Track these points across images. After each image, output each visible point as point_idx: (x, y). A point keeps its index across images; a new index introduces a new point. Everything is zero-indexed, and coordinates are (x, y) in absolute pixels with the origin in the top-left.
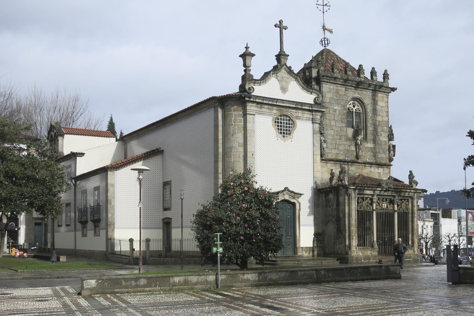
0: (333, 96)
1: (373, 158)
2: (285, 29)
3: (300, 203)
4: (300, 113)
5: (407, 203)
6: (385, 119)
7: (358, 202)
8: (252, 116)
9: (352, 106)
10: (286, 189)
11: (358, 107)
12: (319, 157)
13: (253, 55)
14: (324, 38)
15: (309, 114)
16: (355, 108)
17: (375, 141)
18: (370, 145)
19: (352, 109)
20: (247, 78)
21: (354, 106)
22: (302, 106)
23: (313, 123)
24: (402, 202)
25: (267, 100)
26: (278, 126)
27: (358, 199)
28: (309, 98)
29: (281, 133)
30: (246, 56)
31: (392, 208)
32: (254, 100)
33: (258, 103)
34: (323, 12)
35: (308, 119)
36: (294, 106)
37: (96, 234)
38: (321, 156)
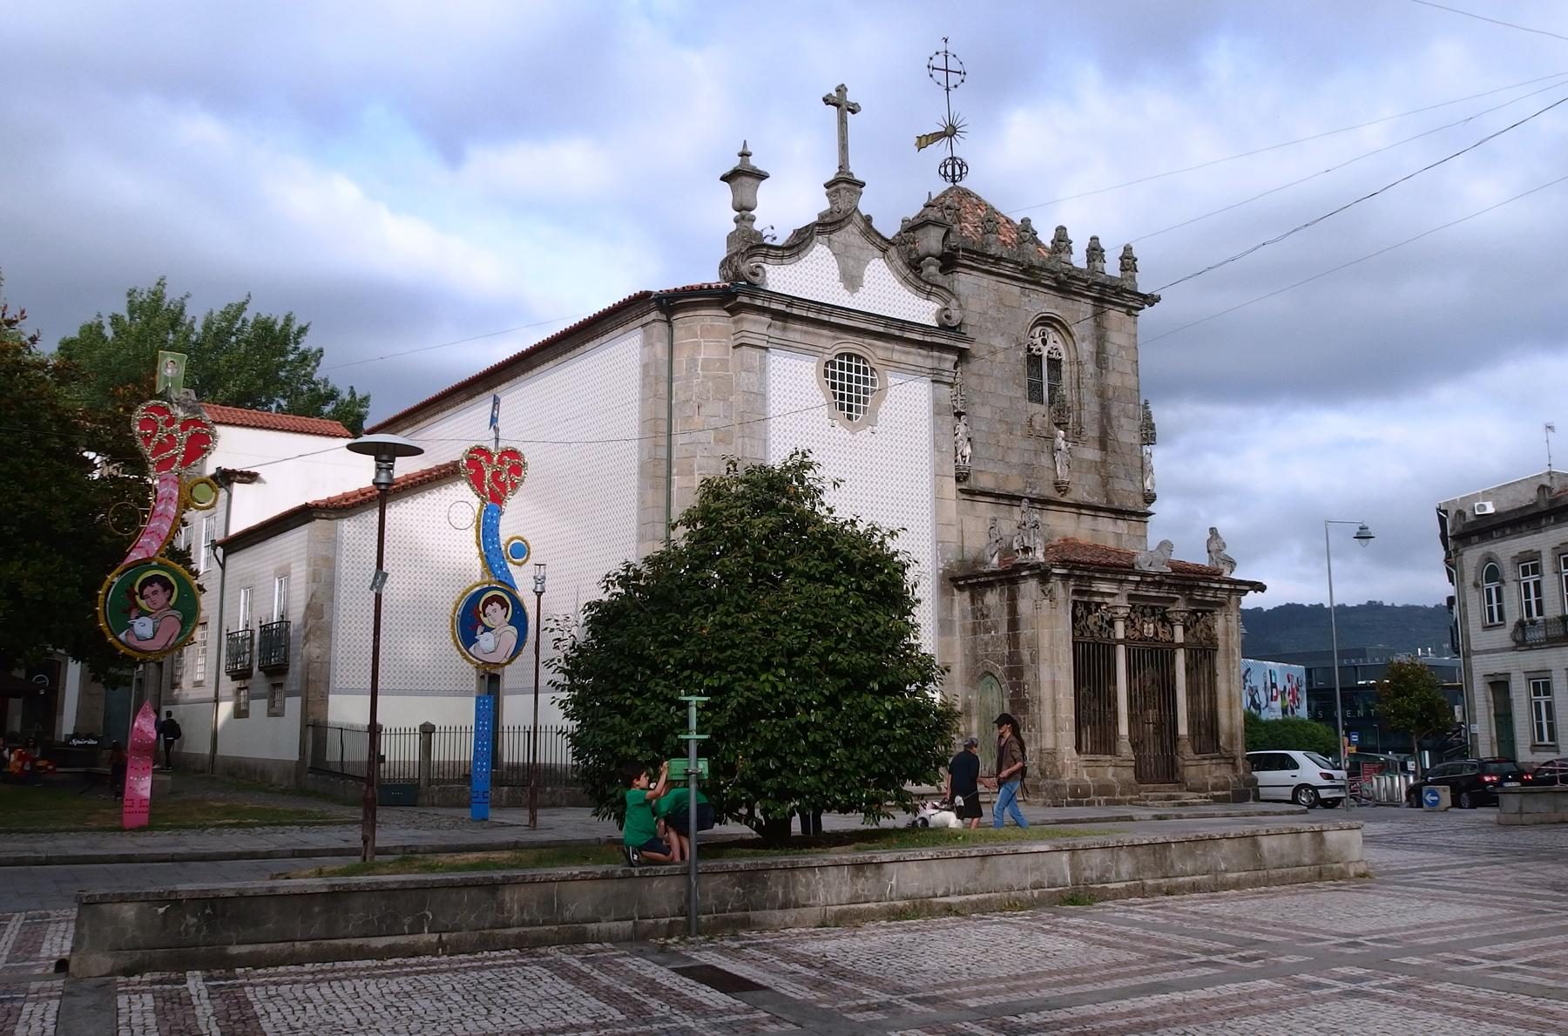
1: (1099, 490)
2: (853, 112)
4: (898, 353)
6: (1130, 382)
7: (1075, 618)
8: (756, 353)
9: (1039, 341)
12: (951, 486)
13: (762, 176)
17: (1103, 443)
18: (1091, 453)
22: (901, 329)
24: (1198, 620)
27: (1075, 603)
28: (923, 311)
30: (743, 176)
31: (1168, 637)
33: (776, 315)
35: (917, 371)
36: (881, 329)
37: (275, 712)
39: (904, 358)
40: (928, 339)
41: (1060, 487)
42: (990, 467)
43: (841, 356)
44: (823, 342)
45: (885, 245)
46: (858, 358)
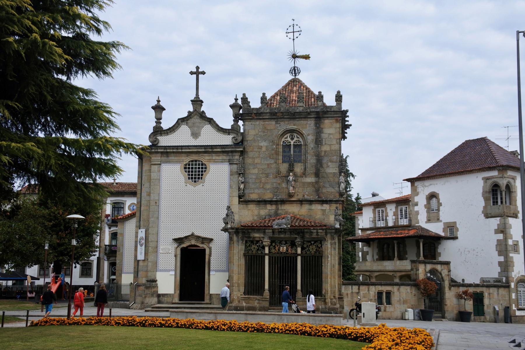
0: (259, 132)
3: (210, 249)
5: (320, 246)
7: (246, 246)
8: (156, 166)
9: (289, 139)
10: (193, 235)
11: (298, 139)
12: (236, 200)
14: (295, 67)
16: (294, 141)
17: (317, 174)
18: (311, 179)
19: (290, 142)
20: (158, 131)
21: (292, 139)
23: (230, 164)
24: (311, 244)
25: (170, 149)
26: (189, 172)
29: (192, 178)
30: (158, 109)
31: (294, 252)
34: (294, 40)
35: (223, 161)
36: (204, 150)
38: (240, 197)
40: (223, 150)
41: (291, 195)
42: (256, 191)
43: (192, 161)
44: (183, 158)
46: (199, 161)
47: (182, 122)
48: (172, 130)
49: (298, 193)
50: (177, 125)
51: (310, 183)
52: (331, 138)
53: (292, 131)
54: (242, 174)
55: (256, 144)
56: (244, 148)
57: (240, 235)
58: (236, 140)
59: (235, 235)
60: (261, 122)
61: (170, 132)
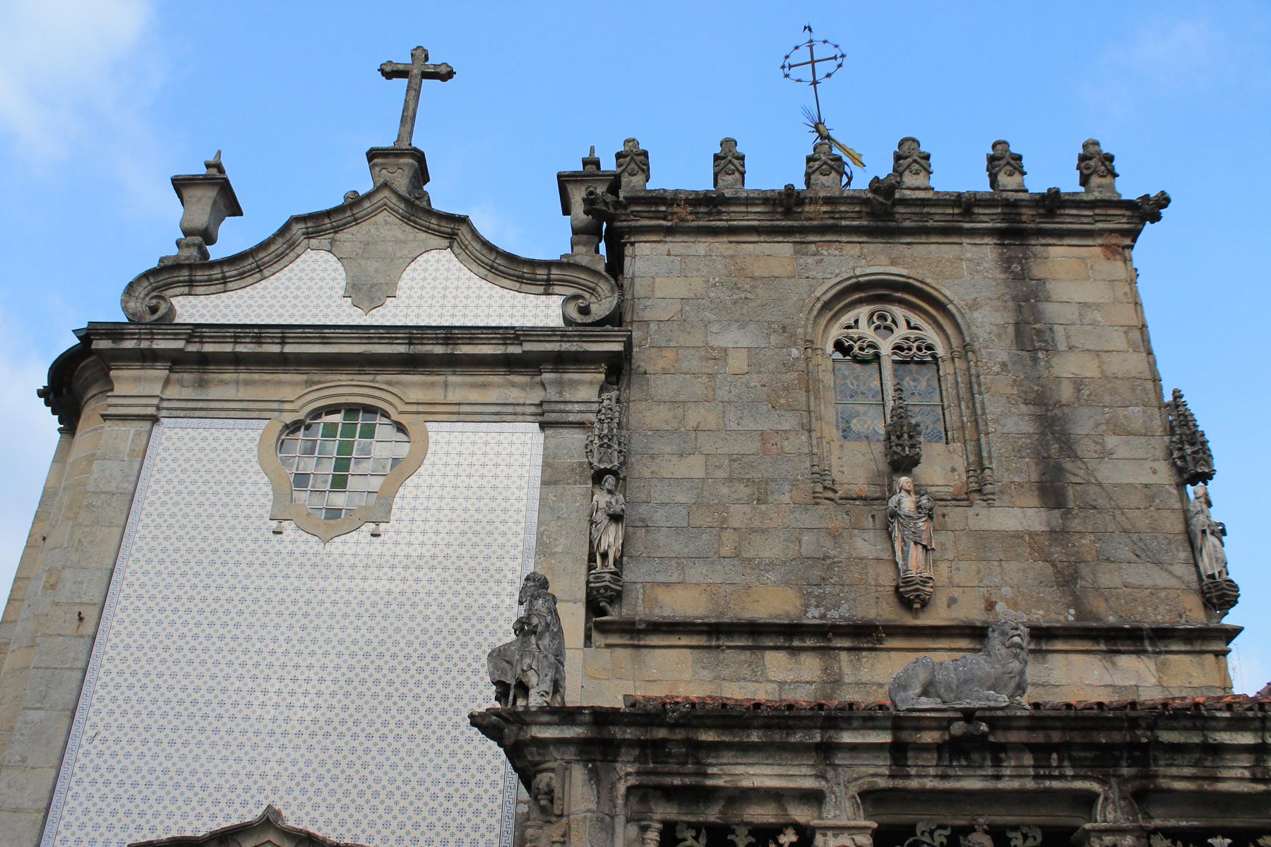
1: (1051, 594)
4: (459, 387)
8: (131, 428)
10: (269, 821)
11: (913, 334)
15: (522, 387)
17: (1052, 491)
18: (1020, 516)
19: (872, 345)
23: (543, 426)
32: (145, 345)
33: (176, 361)
34: (815, 83)
35: (503, 413)
36: (402, 349)
39: (474, 396)
42: (697, 573)
44: (287, 393)
45: (447, 227)
46: (370, 410)
47: (308, 235)
48: (252, 264)
49: (956, 592)
50: (278, 246)
51: (1018, 535)
52: (1094, 323)
53: (879, 292)
54: (614, 473)
55: (696, 339)
56: (629, 345)
57: (626, 771)
58: (585, 311)
59: (578, 774)
60: (720, 246)
61: (242, 276)
